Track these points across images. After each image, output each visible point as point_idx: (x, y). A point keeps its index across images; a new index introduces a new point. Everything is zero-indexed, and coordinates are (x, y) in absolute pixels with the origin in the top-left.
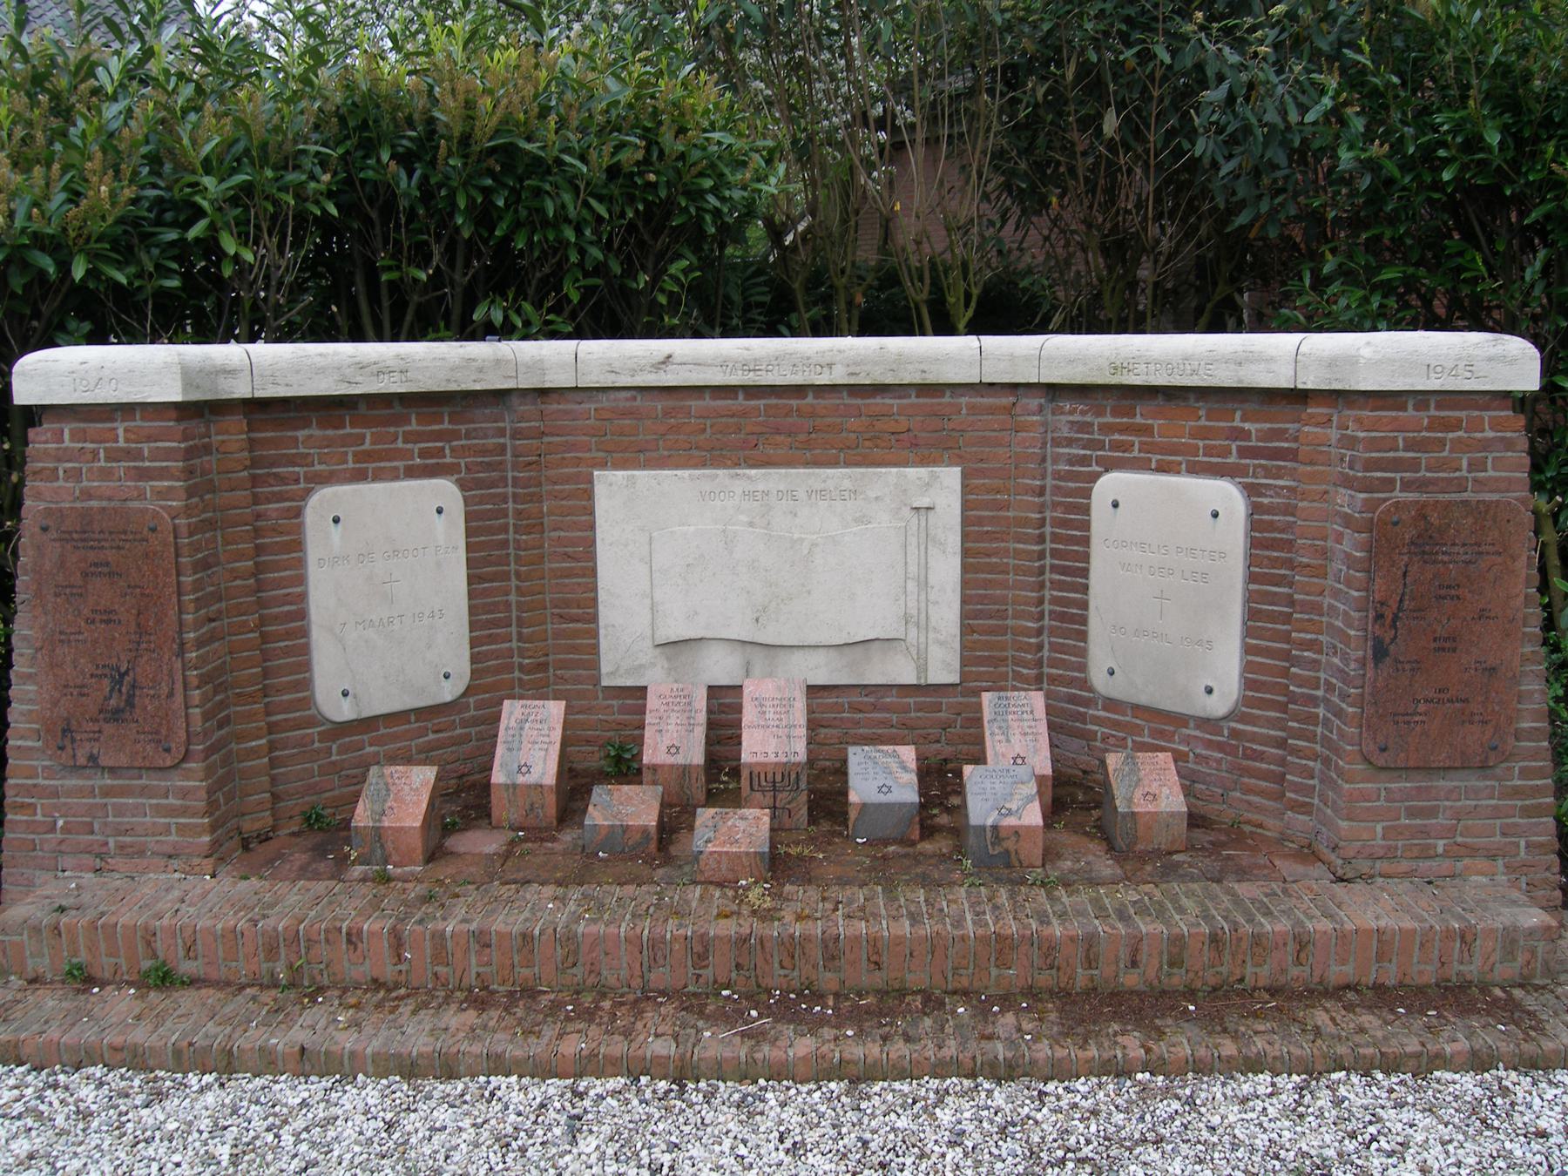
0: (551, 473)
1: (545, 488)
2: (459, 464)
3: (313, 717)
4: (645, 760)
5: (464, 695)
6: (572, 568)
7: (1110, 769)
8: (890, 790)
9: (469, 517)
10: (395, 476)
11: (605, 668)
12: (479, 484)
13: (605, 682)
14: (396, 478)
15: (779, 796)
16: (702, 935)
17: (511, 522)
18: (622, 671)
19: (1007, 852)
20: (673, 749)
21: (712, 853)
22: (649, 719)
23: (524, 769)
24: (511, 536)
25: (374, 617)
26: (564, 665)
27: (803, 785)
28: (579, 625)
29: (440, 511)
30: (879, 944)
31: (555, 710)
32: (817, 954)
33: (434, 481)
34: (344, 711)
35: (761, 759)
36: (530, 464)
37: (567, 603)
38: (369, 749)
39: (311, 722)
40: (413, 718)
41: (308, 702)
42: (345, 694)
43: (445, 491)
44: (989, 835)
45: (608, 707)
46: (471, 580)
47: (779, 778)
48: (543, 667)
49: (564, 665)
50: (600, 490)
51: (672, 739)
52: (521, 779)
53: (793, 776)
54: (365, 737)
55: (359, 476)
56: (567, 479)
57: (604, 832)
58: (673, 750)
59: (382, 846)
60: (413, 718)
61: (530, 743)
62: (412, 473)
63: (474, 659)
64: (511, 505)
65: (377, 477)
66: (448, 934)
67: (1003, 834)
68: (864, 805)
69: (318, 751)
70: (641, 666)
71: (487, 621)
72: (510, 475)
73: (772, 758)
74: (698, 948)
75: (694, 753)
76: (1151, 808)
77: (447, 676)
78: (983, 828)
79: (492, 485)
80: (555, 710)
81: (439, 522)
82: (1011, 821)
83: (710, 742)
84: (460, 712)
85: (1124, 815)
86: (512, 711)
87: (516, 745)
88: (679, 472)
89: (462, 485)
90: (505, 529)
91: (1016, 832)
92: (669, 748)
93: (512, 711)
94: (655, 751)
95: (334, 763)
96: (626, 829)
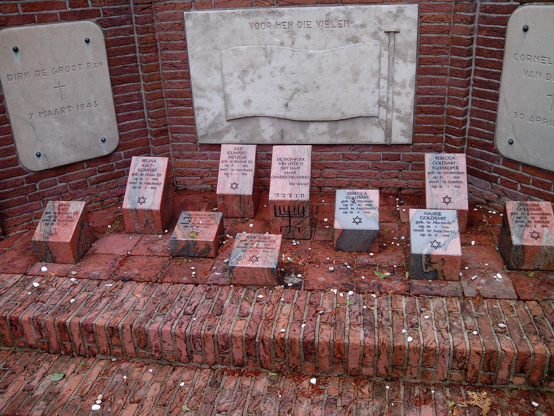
0: (159, 14)
1: (156, 23)
2: (98, 10)
3: (21, 169)
4: (218, 192)
5: (116, 150)
6: (176, 73)
7: (509, 212)
8: (360, 222)
9: (108, 44)
10: (53, 19)
11: (200, 133)
12: (113, 23)
13: (200, 141)
14: (56, 21)
15: (293, 220)
16: (224, 335)
17: (137, 45)
18: (209, 135)
19: (436, 270)
20: (235, 185)
21: (240, 268)
22: (222, 166)
23: (142, 200)
24: (138, 55)
25: (51, 109)
26: (176, 131)
27: (307, 214)
28: (183, 107)
29: (87, 41)
30: (342, 348)
31: (161, 164)
32: (298, 350)
33: (82, 22)
34: (41, 165)
35: (281, 198)
36: (144, 9)
37: (175, 95)
38: (60, 185)
39: (21, 171)
40: (85, 165)
41: (16, 161)
42: (39, 156)
43: (91, 28)
44: (424, 260)
45: (204, 155)
46: (113, 83)
47: (292, 209)
48: (165, 132)
49: (176, 131)
50: (189, 24)
51: (234, 179)
52: (139, 207)
53: (301, 209)
54: (57, 178)
55: (28, 20)
56: (168, 18)
57: (182, 244)
58: (234, 186)
59: (50, 252)
60: (85, 165)
61: (145, 185)
62: (65, 17)
63: (120, 129)
64: (136, 35)
65: (43, 20)
66: (67, 324)
67: (433, 260)
68: (344, 231)
69: (27, 188)
70: (220, 132)
71: (127, 106)
72: (133, 16)
73: (288, 198)
74: (222, 343)
75: (246, 188)
76: (535, 243)
77: (104, 141)
78: (420, 256)
79: (122, 23)
80: (161, 164)
81: (88, 49)
82: (439, 252)
83: (255, 184)
84: (115, 160)
85: (517, 247)
86: (137, 163)
87: (138, 185)
88: (236, 11)
89: (100, 23)
90: (134, 50)
91: (443, 259)
92: (232, 185)
93: (137, 163)
94: (224, 187)
95: (38, 194)
96: (195, 243)
